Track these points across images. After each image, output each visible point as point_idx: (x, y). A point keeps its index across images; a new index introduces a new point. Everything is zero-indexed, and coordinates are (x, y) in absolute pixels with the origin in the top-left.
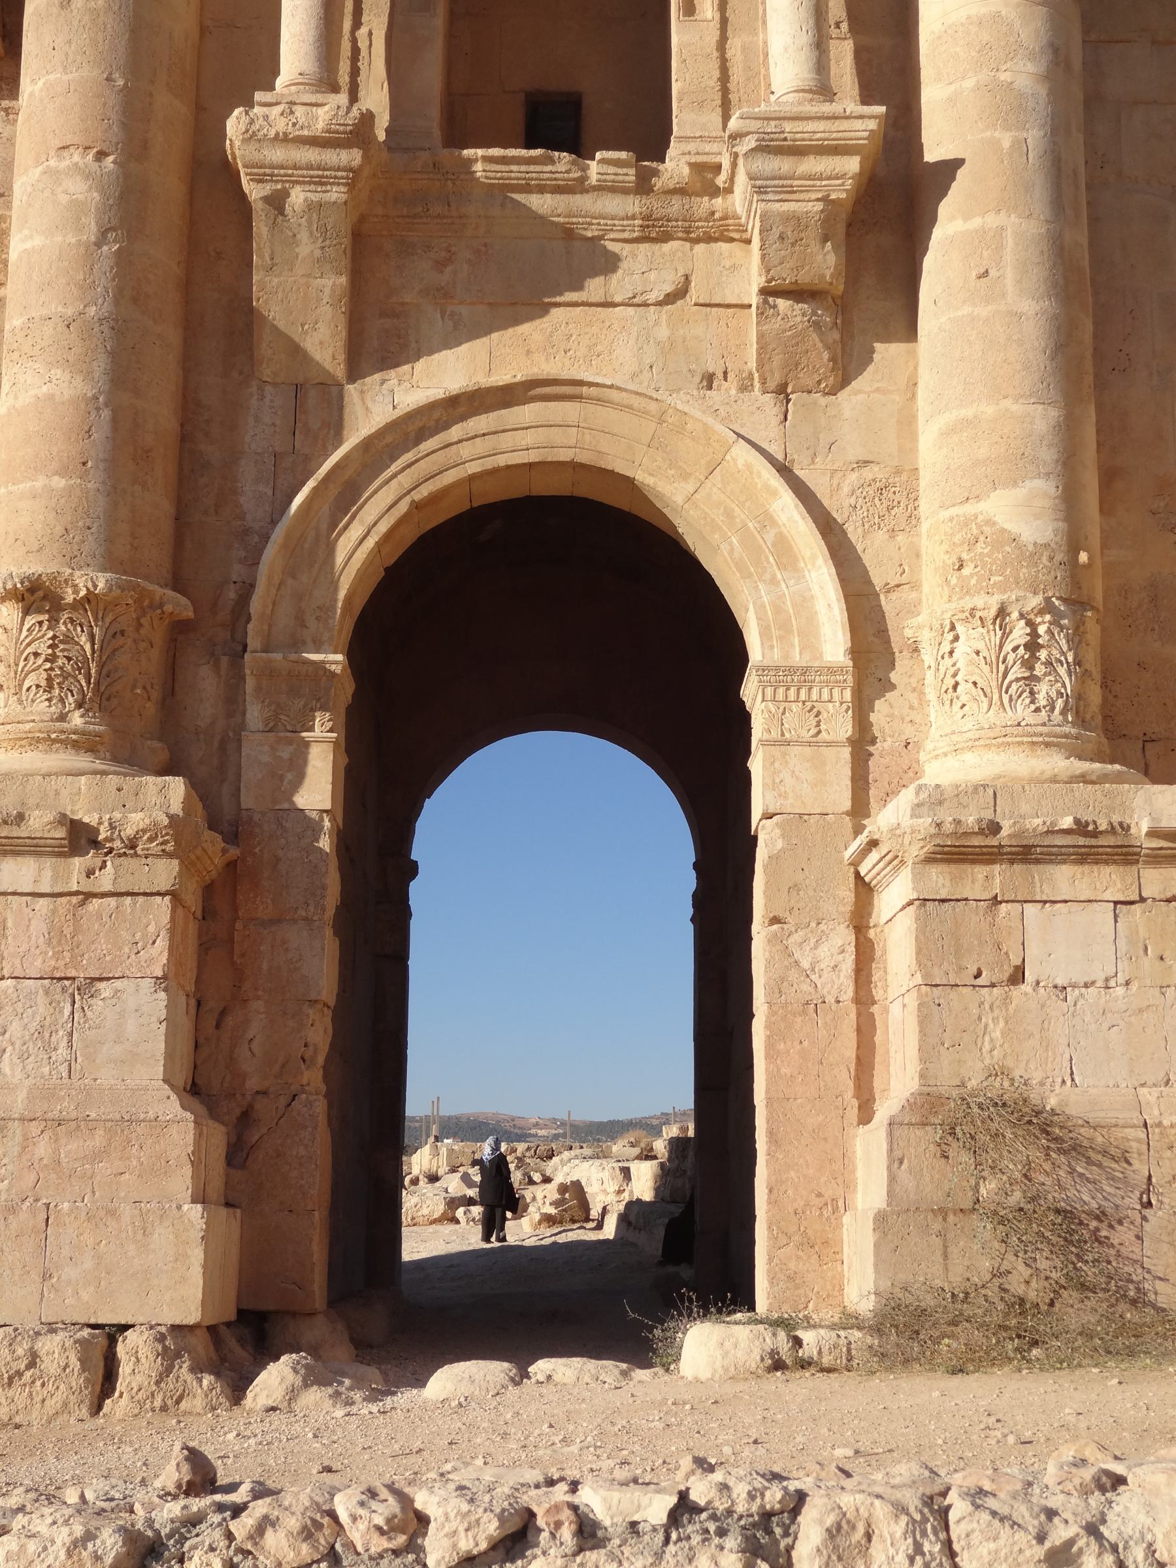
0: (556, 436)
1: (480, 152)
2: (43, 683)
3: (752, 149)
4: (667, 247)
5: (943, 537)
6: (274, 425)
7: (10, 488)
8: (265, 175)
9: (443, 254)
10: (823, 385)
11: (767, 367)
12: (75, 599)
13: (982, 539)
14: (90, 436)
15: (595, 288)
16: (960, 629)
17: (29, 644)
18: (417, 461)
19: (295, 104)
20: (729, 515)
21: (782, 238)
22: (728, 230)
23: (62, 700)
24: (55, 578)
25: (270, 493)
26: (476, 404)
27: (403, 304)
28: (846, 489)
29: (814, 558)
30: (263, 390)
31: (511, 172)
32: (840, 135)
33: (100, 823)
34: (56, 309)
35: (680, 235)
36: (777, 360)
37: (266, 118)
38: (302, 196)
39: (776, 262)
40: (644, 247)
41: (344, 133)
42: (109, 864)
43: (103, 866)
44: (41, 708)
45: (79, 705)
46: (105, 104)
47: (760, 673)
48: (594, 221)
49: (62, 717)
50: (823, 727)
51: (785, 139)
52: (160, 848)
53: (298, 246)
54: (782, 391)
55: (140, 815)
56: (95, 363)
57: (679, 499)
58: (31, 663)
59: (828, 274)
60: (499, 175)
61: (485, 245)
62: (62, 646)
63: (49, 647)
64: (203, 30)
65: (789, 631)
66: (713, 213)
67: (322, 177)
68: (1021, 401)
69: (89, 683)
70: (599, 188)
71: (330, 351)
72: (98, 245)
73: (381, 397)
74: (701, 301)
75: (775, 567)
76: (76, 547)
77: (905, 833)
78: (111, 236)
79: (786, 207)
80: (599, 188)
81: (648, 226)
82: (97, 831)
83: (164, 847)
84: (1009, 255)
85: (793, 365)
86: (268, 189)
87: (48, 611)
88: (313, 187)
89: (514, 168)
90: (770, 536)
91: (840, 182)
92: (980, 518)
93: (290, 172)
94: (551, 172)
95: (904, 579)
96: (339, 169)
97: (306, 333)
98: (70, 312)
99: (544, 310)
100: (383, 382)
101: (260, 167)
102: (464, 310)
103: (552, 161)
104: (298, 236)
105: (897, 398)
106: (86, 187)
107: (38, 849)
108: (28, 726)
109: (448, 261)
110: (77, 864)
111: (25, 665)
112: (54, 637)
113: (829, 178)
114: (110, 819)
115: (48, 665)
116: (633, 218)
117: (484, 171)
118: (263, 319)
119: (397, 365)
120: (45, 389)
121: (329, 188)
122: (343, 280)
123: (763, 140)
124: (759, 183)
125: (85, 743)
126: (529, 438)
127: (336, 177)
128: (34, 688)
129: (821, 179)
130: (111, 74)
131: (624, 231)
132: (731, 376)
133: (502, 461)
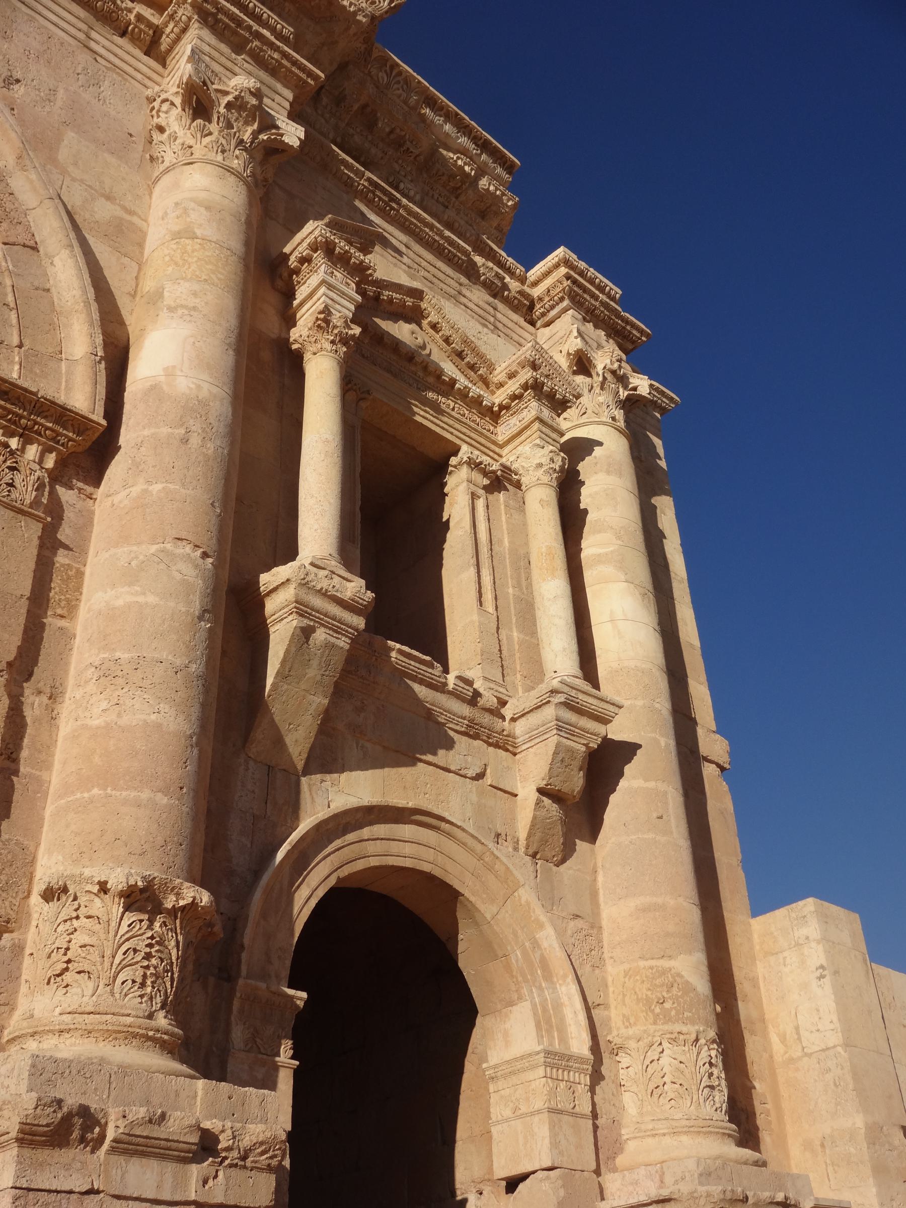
1: (398, 646)
2: (139, 980)
3: (560, 703)
4: (477, 743)
5: (645, 979)
6: (253, 792)
7: (109, 791)
8: (306, 612)
10: (555, 859)
11: (531, 839)
12: (174, 906)
13: (676, 985)
14: (186, 767)
15: (442, 756)
16: (666, 1045)
17: (128, 940)
18: (343, 847)
19: (334, 573)
20: (515, 934)
21: (562, 761)
22: (507, 744)
23: (151, 999)
24: (166, 883)
25: (249, 845)
26: (381, 815)
28: (569, 932)
29: (565, 976)
30: (248, 764)
31: (410, 665)
32: (603, 711)
33: (223, 1131)
34: (167, 656)
35: (485, 738)
36: (538, 835)
37: (316, 575)
38: (324, 636)
39: (555, 775)
41: (361, 605)
42: (221, 1174)
43: (216, 1177)
44: (133, 1003)
45: (162, 1008)
46: (210, 521)
47: (546, 1055)
48: (445, 713)
49: (150, 1016)
50: (577, 1102)
51: (578, 703)
52: (267, 1162)
53: (308, 668)
54: (534, 856)
55: (261, 1127)
56: (192, 709)
57: (488, 916)
58: (130, 958)
59: (577, 789)
60: (404, 664)
61: (383, 706)
62: (157, 948)
63: (147, 946)
65: (551, 1026)
66: (503, 731)
67: (339, 628)
68: (688, 900)
69: (172, 987)
70: (450, 693)
71: (300, 748)
72: (201, 618)
73: (321, 793)
74: (494, 784)
75: (541, 978)
76: (171, 859)
77: (701, 1196)
78: (207, 616)
79: (569, 743)
80: (450, 693)
81: (470, 727)
82: (218, 1141)
83: (270, 1161)
84: (671, 811)
85: (544, 842)
86: (306, 622)
87: (147, 912)
88: (331, 632)
89: (412, 663)
90: (538, 955)
91: (595, 738)
92: (673, 971)
93: (322, 617)
94: (431, 673)
95: (601, 1001)
96: (350, 627)
97: (290, 731)
98: (178, 662)
99: (413, 761)
100: (322, 781)
101: (305, 606)
102: (368, 745)
103: (432, 667)
104: (311, 662)
105: (588, 879)
106: (195, 574)
107: (167, 1152)
108: (129, 1020)
110: (196, 1173)
111: (124, 959)
112: (152, 938)
113: (591, 734)
114: (232, 1128)
115: (146, 963)
116: (464, 718)
117: (396, 658)
118: (267, 710)
119: (330, 772)
120: (153, 717)
121: (340, 636)
122: (326, 701)
123: (568, 699)
124: (560, 724)
125: (168, 1047)
126: (408, 849)
127: (347, 631)
128: (130, 982)
129: (588, 733)
130: (214, 502)
131: (458, 725)
132: (509, 838)
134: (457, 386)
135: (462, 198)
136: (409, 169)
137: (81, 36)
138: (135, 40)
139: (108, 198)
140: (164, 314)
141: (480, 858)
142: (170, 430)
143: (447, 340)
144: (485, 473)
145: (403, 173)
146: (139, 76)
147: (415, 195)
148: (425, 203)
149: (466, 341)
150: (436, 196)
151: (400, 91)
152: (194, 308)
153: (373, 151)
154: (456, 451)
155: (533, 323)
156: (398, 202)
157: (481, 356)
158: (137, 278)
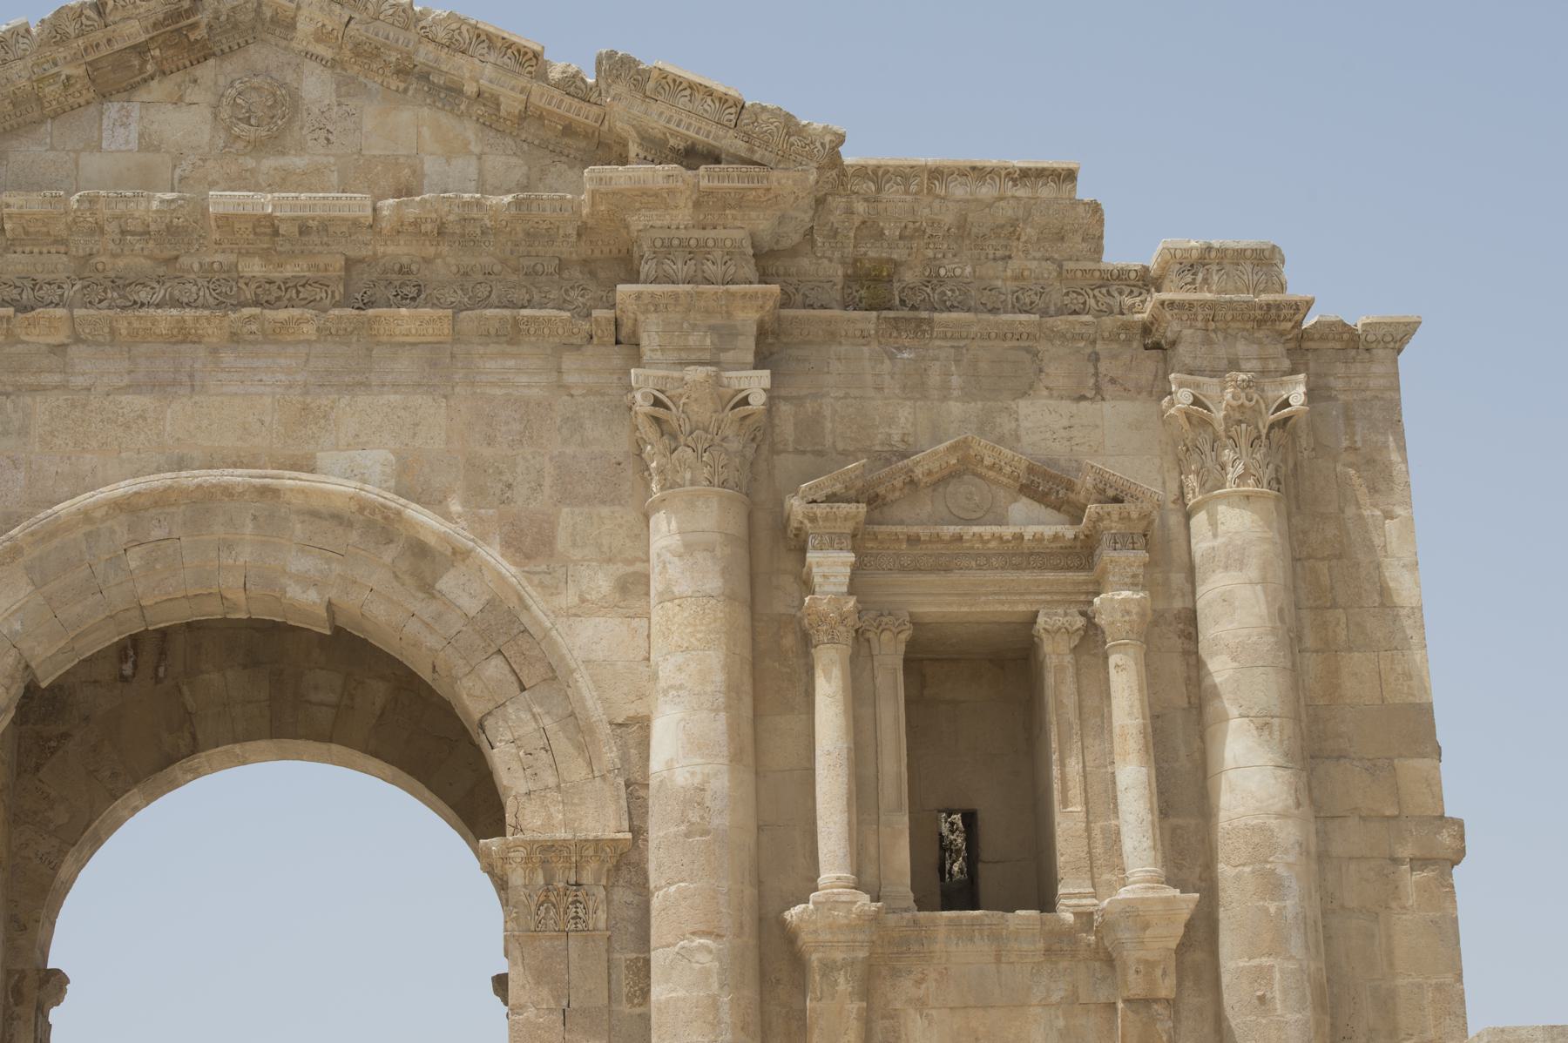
9: (920, 975)
27: (896, 1010)
61: (946, 969)
64: (759, 828)
102: (934, 1012)
109: (923, 980)
122: (865, 1004)
134: (1026, 538)
135: (1023, 238)
136: (945, 246)
140: (661, 699)
142: (676, 829)
145: (940, 256)
147: (963, 270)
148: (977, 274)
150: (991, 252)
151: (895, 187)
152: (681, 687)
153: (895, 256)
157: (1053, 477)
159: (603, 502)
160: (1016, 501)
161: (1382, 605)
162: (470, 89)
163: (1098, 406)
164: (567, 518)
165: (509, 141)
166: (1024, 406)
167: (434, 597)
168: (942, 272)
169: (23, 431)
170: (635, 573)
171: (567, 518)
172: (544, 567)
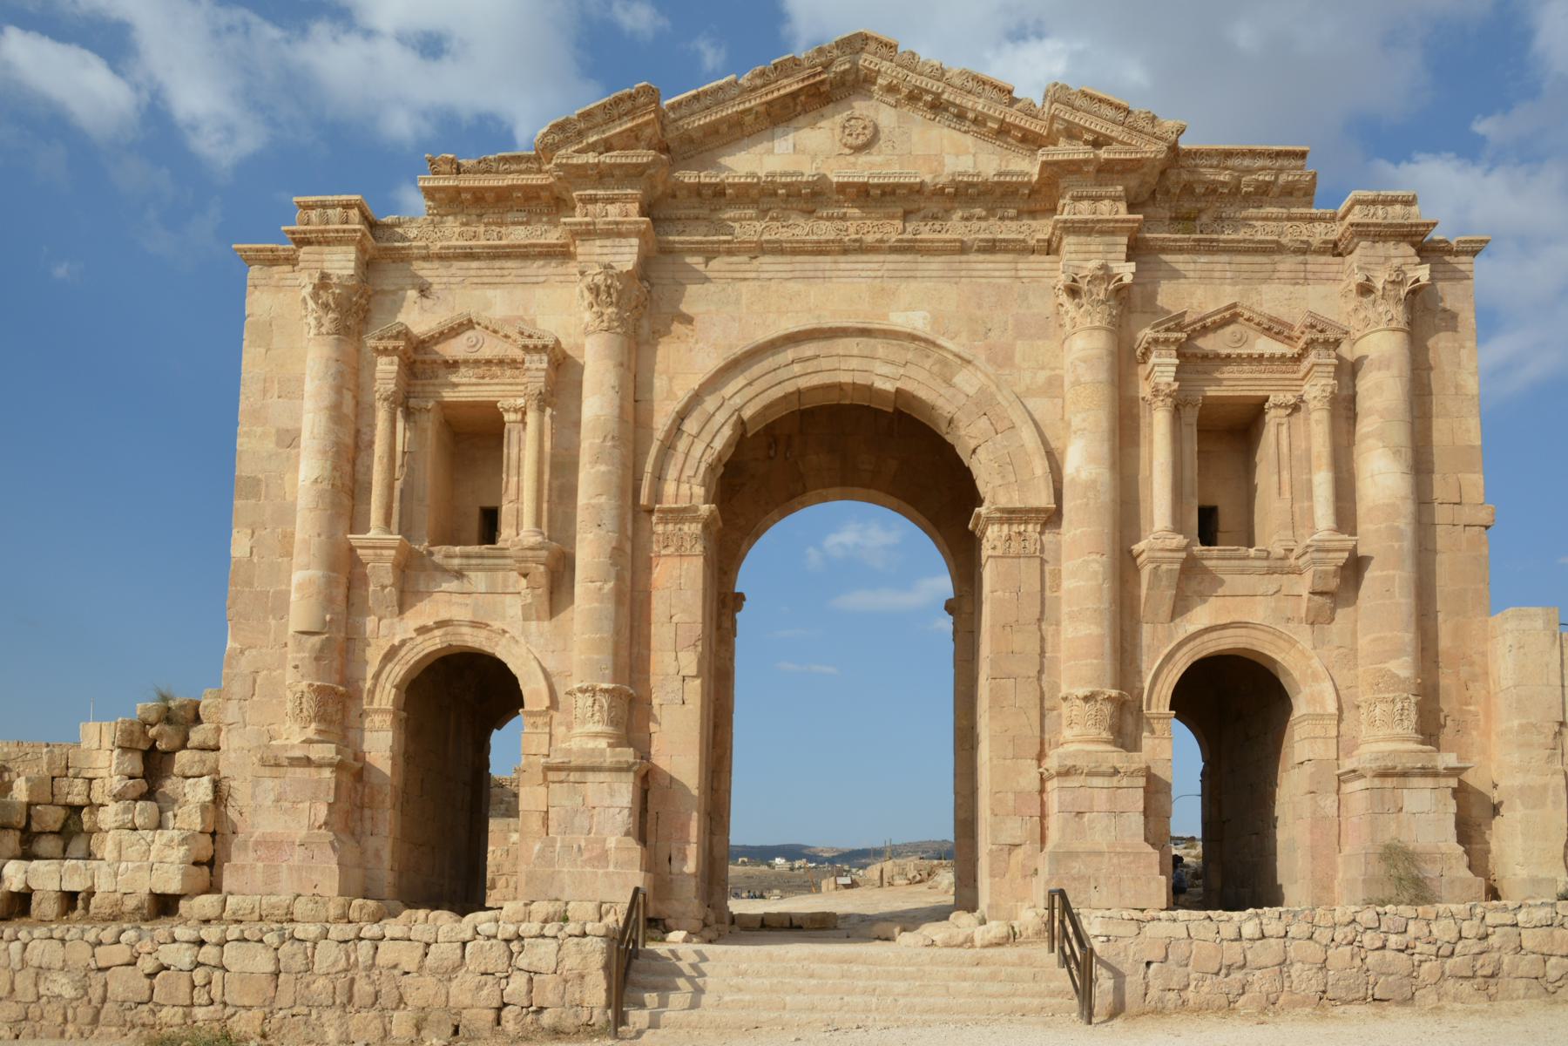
0: (1239, 639)
40: (1268, 576)
54: (1312, 624)
90: (1309, 671)
126: (1230, 640)
133: (1221, 648)
135: (1270, 195)
137: (1013, 273)
138: (1040, 252)
139: (1043, 368)
141: (1274, 634)
143: (1259, 324)
144: (1286, 407)
146: (1046, 273)
149: (1271, 319)
154: (1266, 399)
155: (1340, 255)
156: (1217, 241)
158: (1063, 407)
159: (1039, 338)
160: (1259, 338)
161: (1457, 394)
162: (971, 115)
163: (1305, 287)
164: (1020, 346)
165: (990, 146)
166: (1264, 288)
167: (951, 386)
168: (1224, 215)
169: (737, 302)
170: (1057, 375)
171: (1020, 346)
172: (1007, 372)
